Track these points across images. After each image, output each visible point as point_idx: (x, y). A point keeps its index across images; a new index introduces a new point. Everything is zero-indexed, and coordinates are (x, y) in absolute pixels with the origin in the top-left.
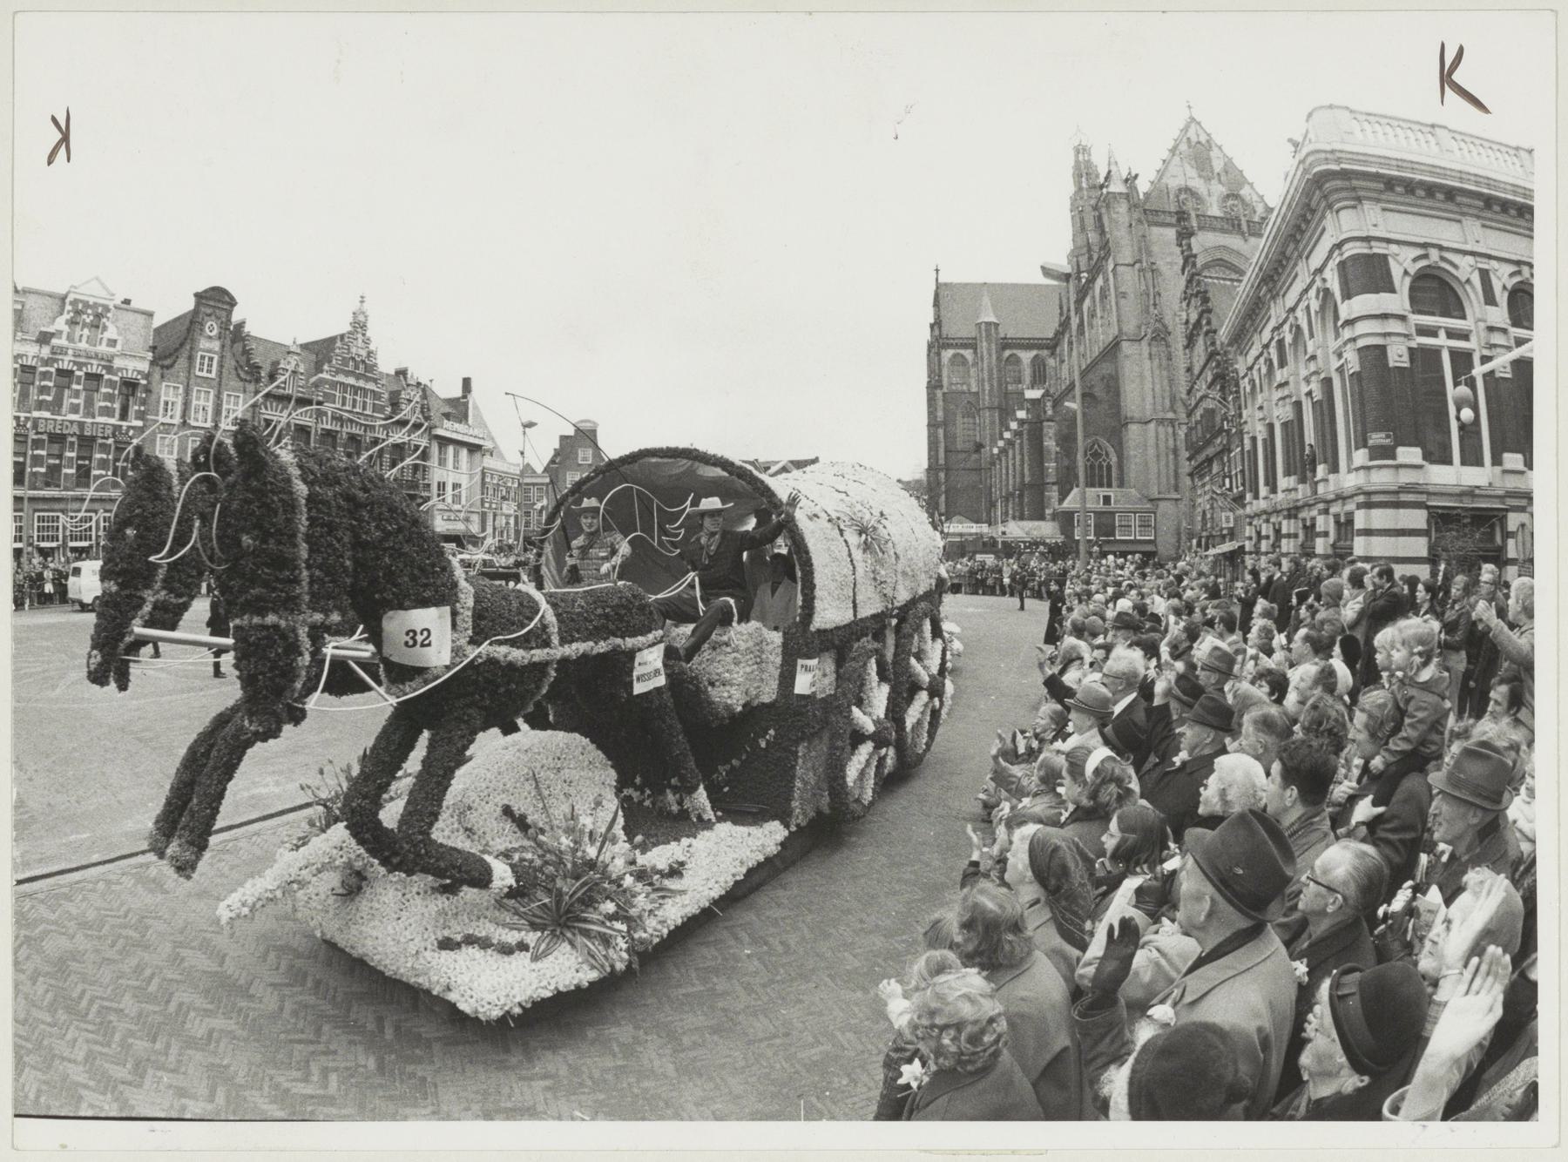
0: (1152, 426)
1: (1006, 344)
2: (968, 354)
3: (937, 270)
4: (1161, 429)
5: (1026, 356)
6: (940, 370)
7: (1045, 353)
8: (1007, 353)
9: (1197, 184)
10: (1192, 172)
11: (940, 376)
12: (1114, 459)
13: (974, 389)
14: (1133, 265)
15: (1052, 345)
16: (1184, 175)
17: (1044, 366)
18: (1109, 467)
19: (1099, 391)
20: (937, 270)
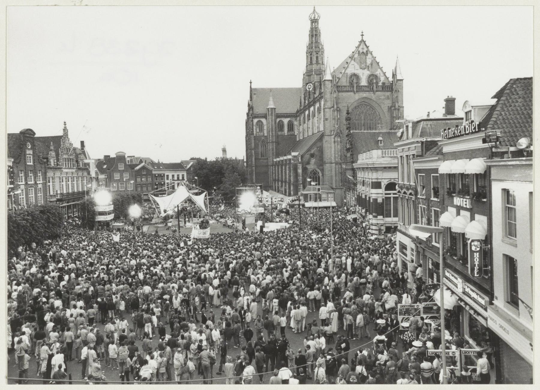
0: (334, 164)
1: (278, 116)
2: (264, 120)
3: (251, 83)
4: (337, 166)
5: (286, 121)
6: (253, 127)
7: (293, 119)
8: (278, 120)
9: (359, 72)
10: (357, 67)
11: (253, 130)
12: (320, 174)
13: (266, 135)
14: (330, 108)
15: (296, 115)
16: (353, 68)
17: (293, 124)
18: (319, 177)
19: (316, 153)
20: (251, 83)
